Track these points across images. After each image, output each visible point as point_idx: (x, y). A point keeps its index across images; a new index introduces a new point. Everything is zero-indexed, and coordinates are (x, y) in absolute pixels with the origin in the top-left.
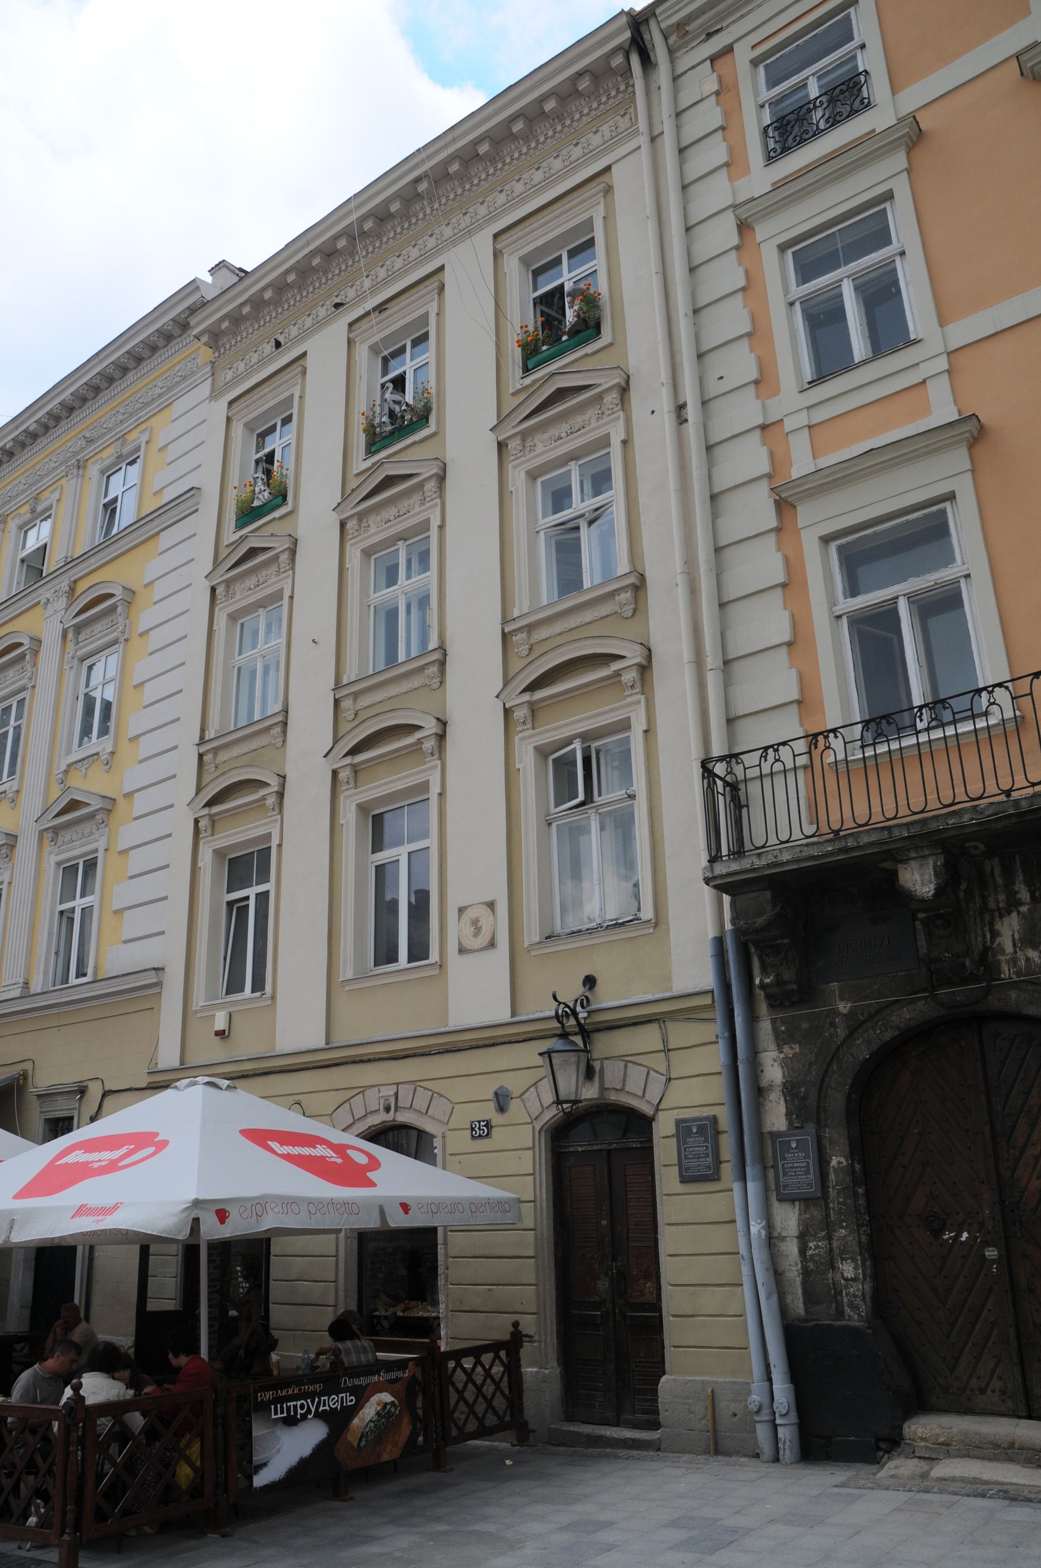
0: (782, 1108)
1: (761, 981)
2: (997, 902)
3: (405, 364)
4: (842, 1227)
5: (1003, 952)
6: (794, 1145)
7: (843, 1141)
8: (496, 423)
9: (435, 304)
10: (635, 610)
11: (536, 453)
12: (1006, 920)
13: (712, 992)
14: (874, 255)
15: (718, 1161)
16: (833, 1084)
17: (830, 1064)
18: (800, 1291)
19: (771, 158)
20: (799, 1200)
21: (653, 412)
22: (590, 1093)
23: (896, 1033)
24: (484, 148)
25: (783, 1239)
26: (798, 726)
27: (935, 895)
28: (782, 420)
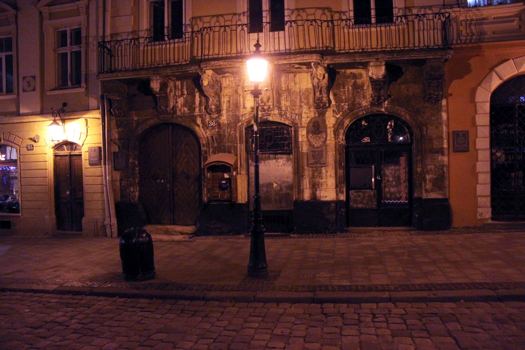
5: (178, 107)
6: (120, 155)
12: (180, 99)
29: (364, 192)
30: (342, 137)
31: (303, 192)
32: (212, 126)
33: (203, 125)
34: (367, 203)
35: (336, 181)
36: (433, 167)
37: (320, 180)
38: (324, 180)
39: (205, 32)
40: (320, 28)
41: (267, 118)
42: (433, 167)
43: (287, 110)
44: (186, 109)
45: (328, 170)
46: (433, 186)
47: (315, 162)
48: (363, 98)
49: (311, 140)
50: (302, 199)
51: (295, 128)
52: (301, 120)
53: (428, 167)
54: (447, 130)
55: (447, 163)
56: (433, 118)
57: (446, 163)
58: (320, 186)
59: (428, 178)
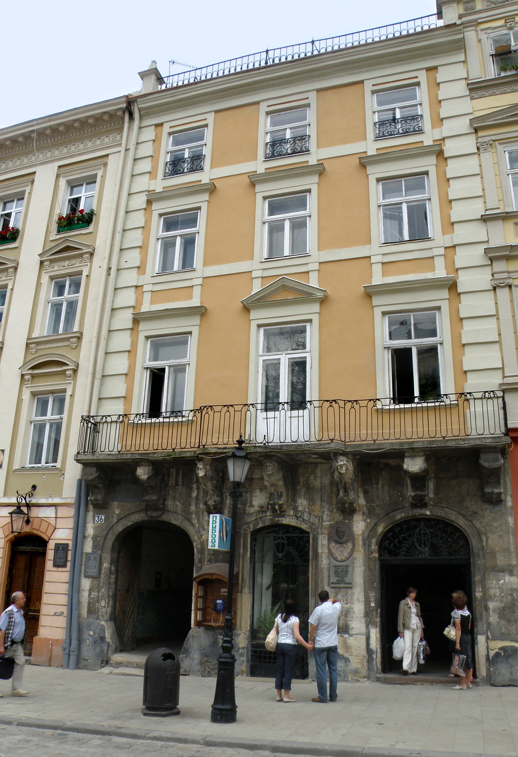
3: (12, 209)
6: (92, 558)
7: (109, 558)
8: (41, 252)
9: (29, 187)
10: (77, 346)
11: (54, 269)
14: (190, 230)
15: (66, 561)
16: (109, 538)
17: (109, 530)
19: (166, 176)
20: (91, 578)
21: (100, 267)
22: (27, 529)
24: (61, 128)
25: (84, 590)
28: (143, 286)
30: (374, 547)
36: (498, 592)
39: (204, 412)
40: (342, 410)
42: (498, 592)
46: (499, 618)
47: (337, 581)
49: (333, 551)
51: (314, 535)
56: (495, 524)
59: (491, 607)
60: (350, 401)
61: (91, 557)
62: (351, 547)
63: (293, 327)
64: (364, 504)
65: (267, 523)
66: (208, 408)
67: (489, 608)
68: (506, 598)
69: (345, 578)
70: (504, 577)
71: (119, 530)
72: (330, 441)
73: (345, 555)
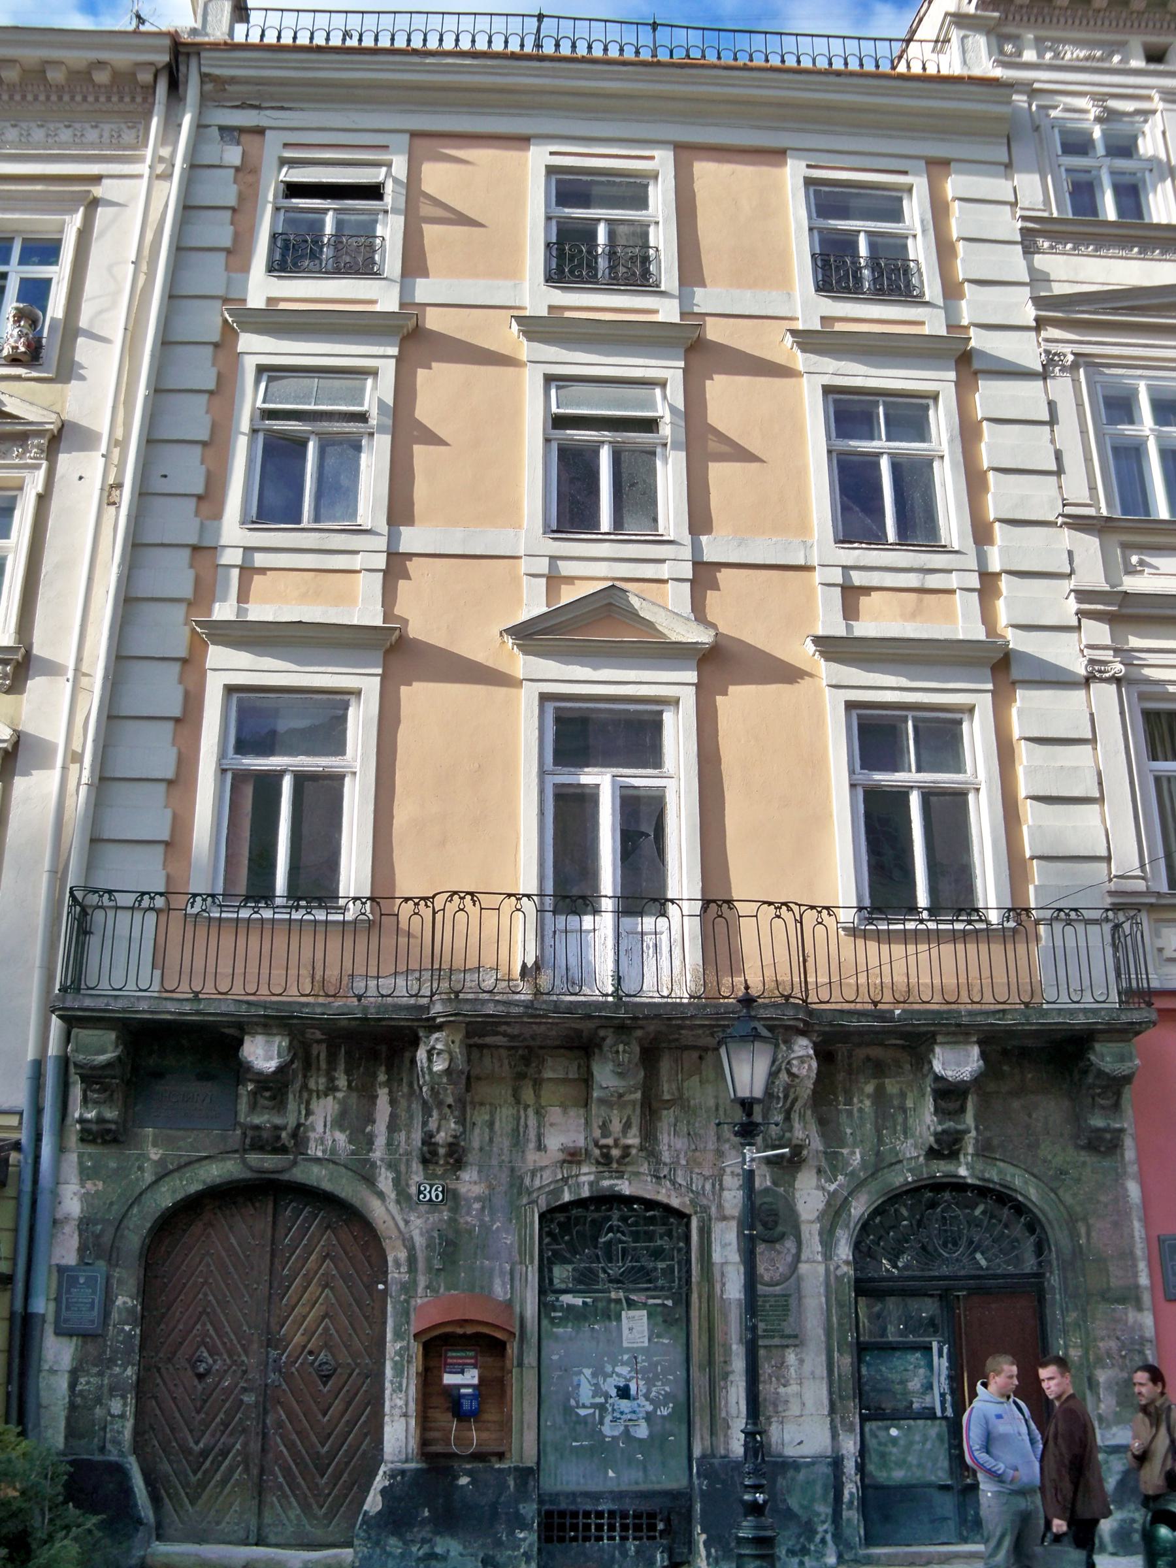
0: (75, 1242)
1: (81, 1114)
2: (317, 1083)
4: (116, 1365)
5: (314, 1130)
6: (82, 1281)
12: (322, 1101)
13: (21, 1114)
16: (131, 1227)
17: (131, 1206)
18: (62, 1425)
20: (78, 1335)
21: (81, 478)
23: (200, 1187)
26: (161, 867)
27: (274, 1073)
29: (909, 1427)
30: (844, 1251)
31: (728, 1427)
32: (431, 1200)
33: (397, 1195)
34: (919, 1465)
35: (831, 1393)
36: (1113, 1344)
37: (782, 1390)
38: (793, 1388)
41: (612, 1186)
43: (678, 1163)
44: (341, 1138)
45: (804, 1355)
48: (905, 1133)
50: (723, 1452)
52: (720, 1196)
53: (1101, 1345)
54: (1143, 1232)
55: (1153, 1333)
57: (1150, 1332)
58: (780, 1409)
60: (812, 908)
61: (77, 1278)
62: (794, 1251)
63: (628, 711)
64: (821, 1148)
65: (585, 1193)
66: (463, 898)
67: (1098, 1384)
68: (1131, 1360)
69: (785, 1323)
70: (1126, 1314)
71: (164, 1205)
72: (782, 1001)
73: (781, 1270)
